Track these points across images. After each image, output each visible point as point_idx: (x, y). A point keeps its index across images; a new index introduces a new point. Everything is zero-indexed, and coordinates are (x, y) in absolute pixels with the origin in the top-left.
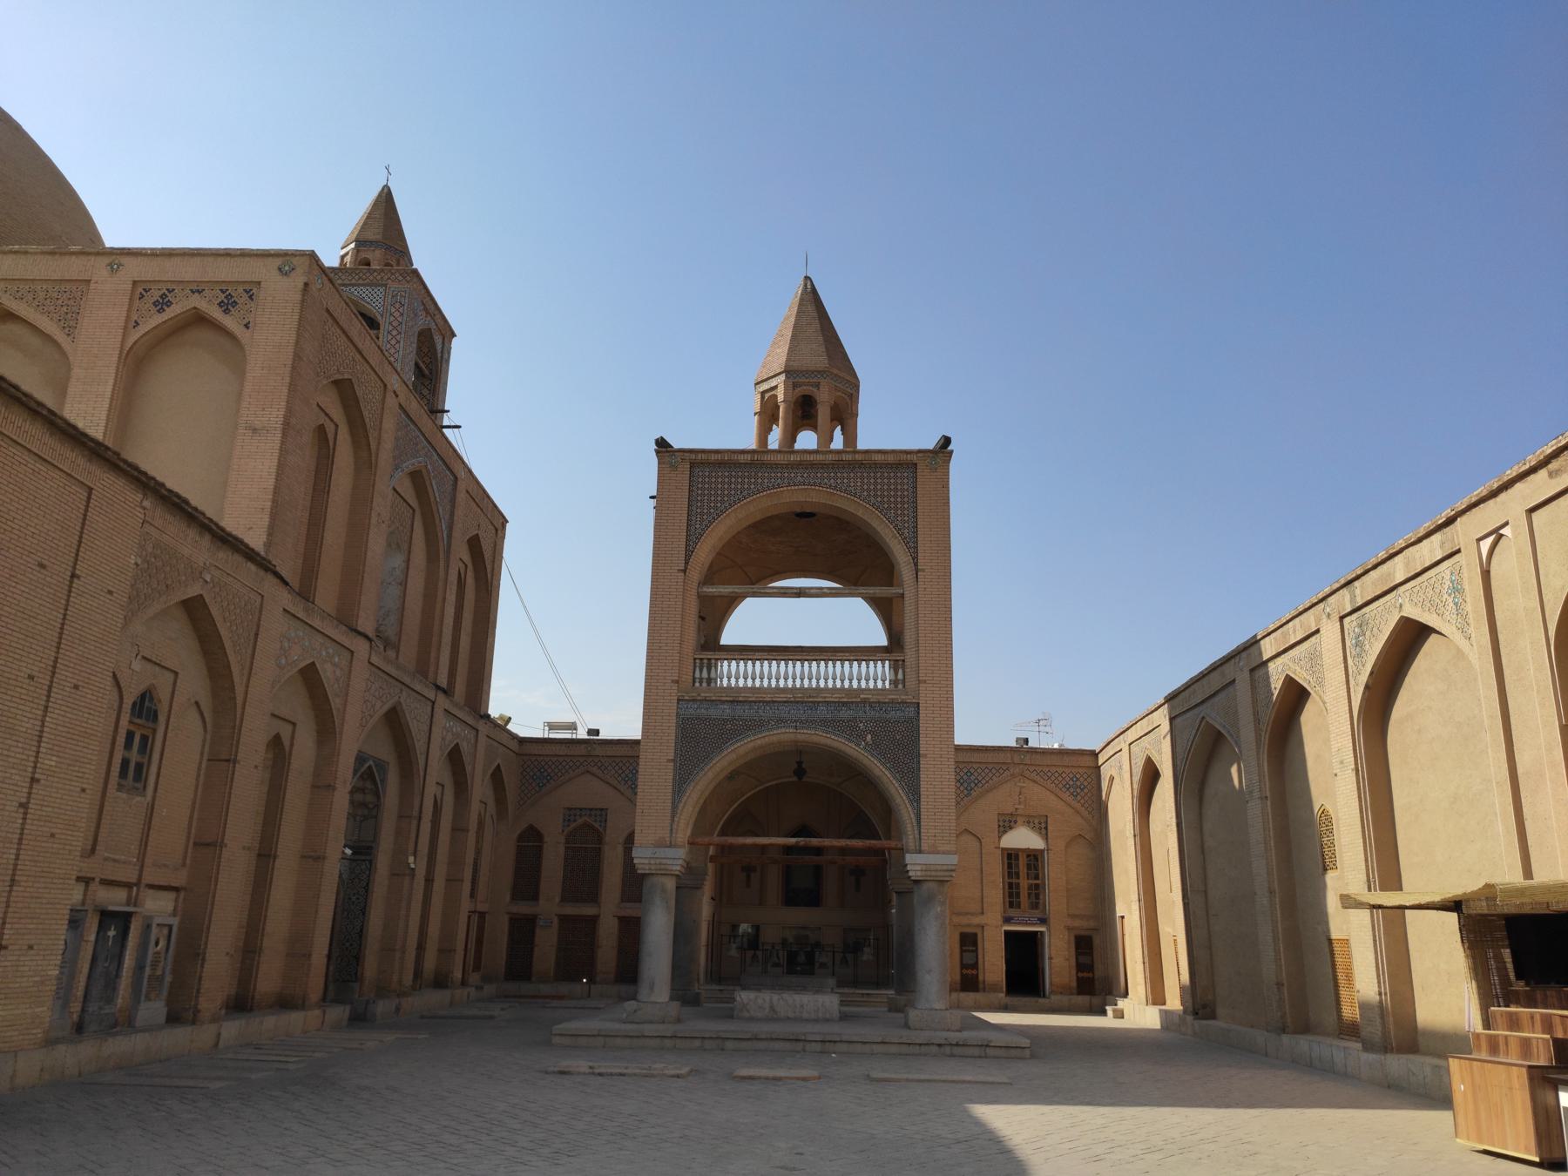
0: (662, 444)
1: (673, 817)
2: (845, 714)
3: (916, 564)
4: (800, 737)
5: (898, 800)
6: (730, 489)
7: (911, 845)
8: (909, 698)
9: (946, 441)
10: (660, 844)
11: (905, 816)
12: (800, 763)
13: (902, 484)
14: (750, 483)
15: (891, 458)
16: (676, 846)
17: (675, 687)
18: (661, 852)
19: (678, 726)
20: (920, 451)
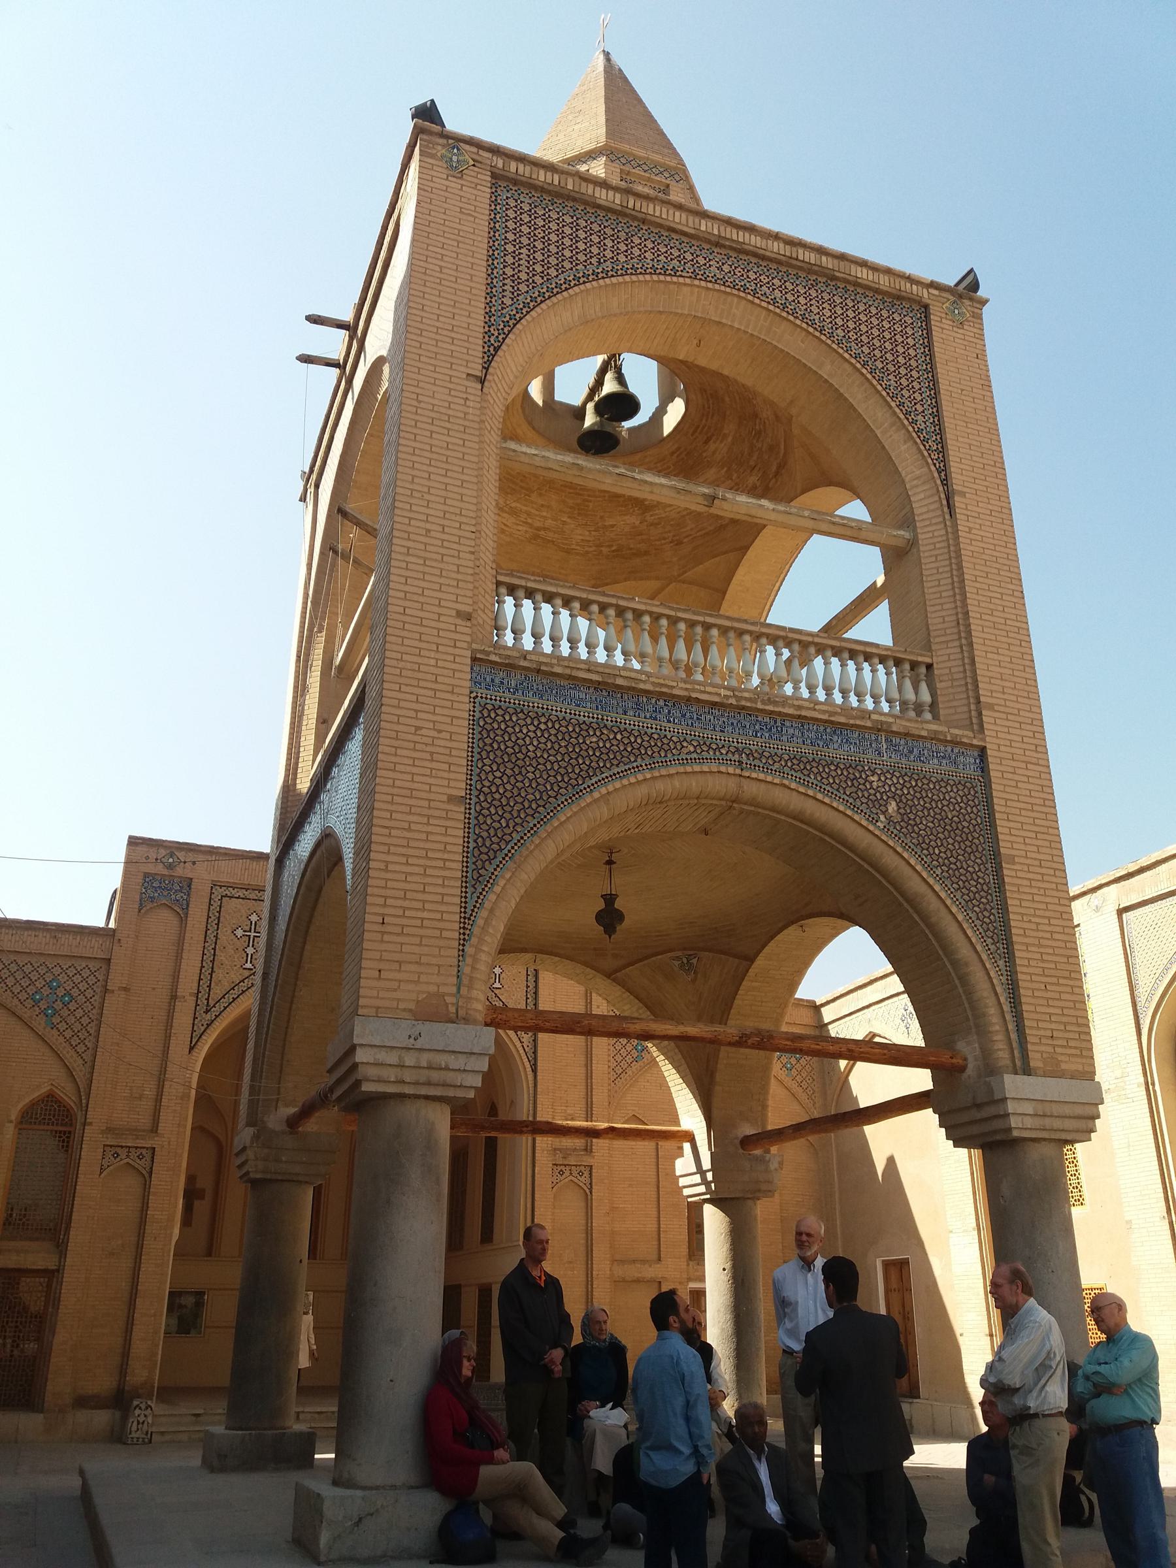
0: (427, 114)
1: (463, 941)
2: (838, 751)
3: (946, 482)
4: (751, 789)
5: (964, 952)
6: (574, 249)
7: (1002, 1055)
8: (965, 735)
9: (970, 285)
10: (431, 1012)
11: (982, 989)
12: (609, 899)
13: (903, 334)
14: (616, 251)
15: (884, 282)
16: (467, 1020)
17: (464, 627)
18: (435, 1034)
19: (473, 722)
20: (933, 285)
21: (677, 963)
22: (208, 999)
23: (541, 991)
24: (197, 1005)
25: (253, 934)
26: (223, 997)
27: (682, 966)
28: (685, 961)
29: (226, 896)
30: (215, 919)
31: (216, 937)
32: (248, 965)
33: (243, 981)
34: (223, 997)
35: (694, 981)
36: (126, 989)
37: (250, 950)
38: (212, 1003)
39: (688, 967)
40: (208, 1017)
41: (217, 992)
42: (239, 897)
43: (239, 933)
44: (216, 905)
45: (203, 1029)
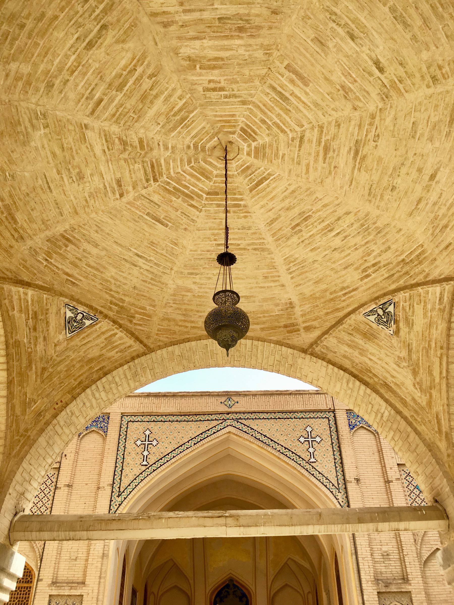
21: (372, 318)
22: (119, 488)
23: (345, 461)
24: (112, 492)
25: (147, 443)
26: (129, 485)
27: (379, 320)
28: (380, 312)
29: (131, 421)
30: (123, 436)
31: (125, 447)
32: (145, 463)
33: (141, 473)
34: (129, 485)
35: (397, 332)
36: (68, 486)
37: (146, 453)
38: (122, 490)
39: (386, 319)
40: (119, 499)
41: (125, 482)
42: (138, 421)
43: (139, 443)
44: (124, 427)
45: (116, 507)
